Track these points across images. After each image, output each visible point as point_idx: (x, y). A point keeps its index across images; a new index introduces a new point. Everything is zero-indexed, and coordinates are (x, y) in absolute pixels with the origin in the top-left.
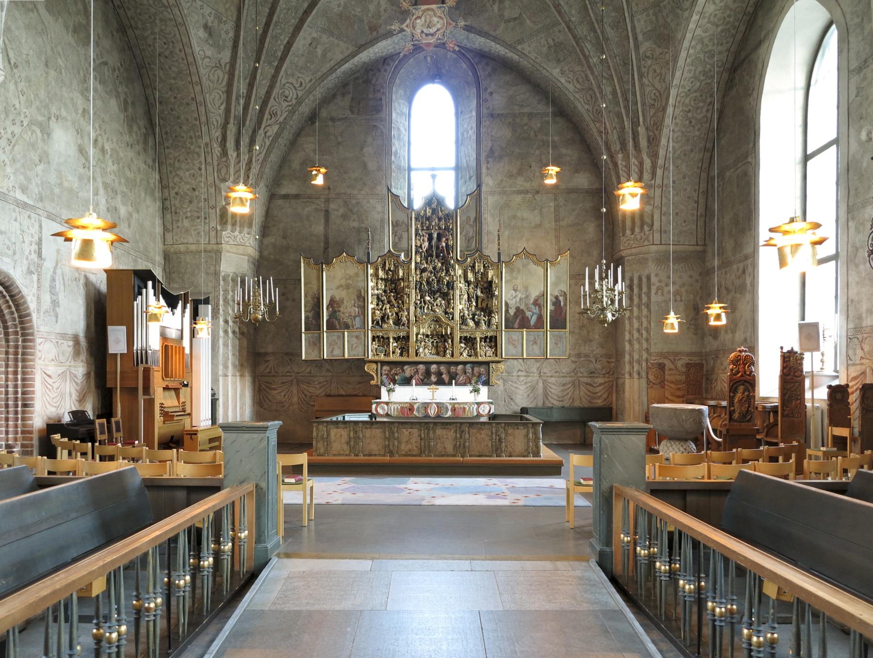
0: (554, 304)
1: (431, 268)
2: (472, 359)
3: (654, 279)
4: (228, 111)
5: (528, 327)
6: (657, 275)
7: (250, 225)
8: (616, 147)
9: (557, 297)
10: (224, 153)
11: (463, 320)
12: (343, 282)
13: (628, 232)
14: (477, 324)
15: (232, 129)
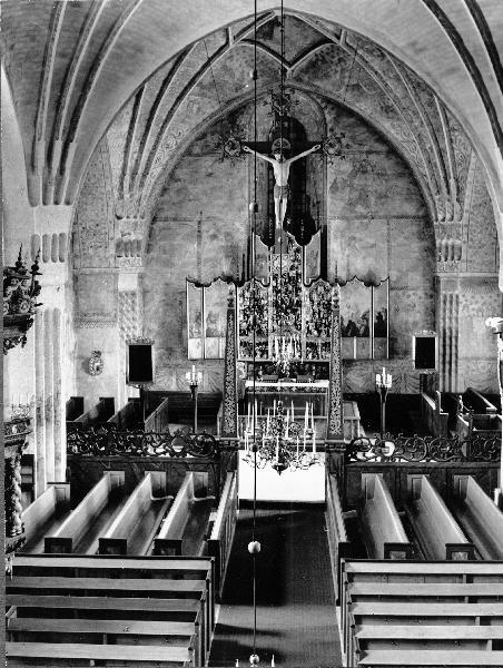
0: (377, 318)
1: (284, 290)
2: (315, 360)
3: (461, 299)
4: (125, 166)
5: (358, 336)
6: (464, 296)
7: (139, 248)
8: (434, 191)
9: (379, 313)
10: (121, 197)
11: (309, 332)
12: (218, 300)
13: (443, 259)
14: (319, 332)
15: (127, 177)
